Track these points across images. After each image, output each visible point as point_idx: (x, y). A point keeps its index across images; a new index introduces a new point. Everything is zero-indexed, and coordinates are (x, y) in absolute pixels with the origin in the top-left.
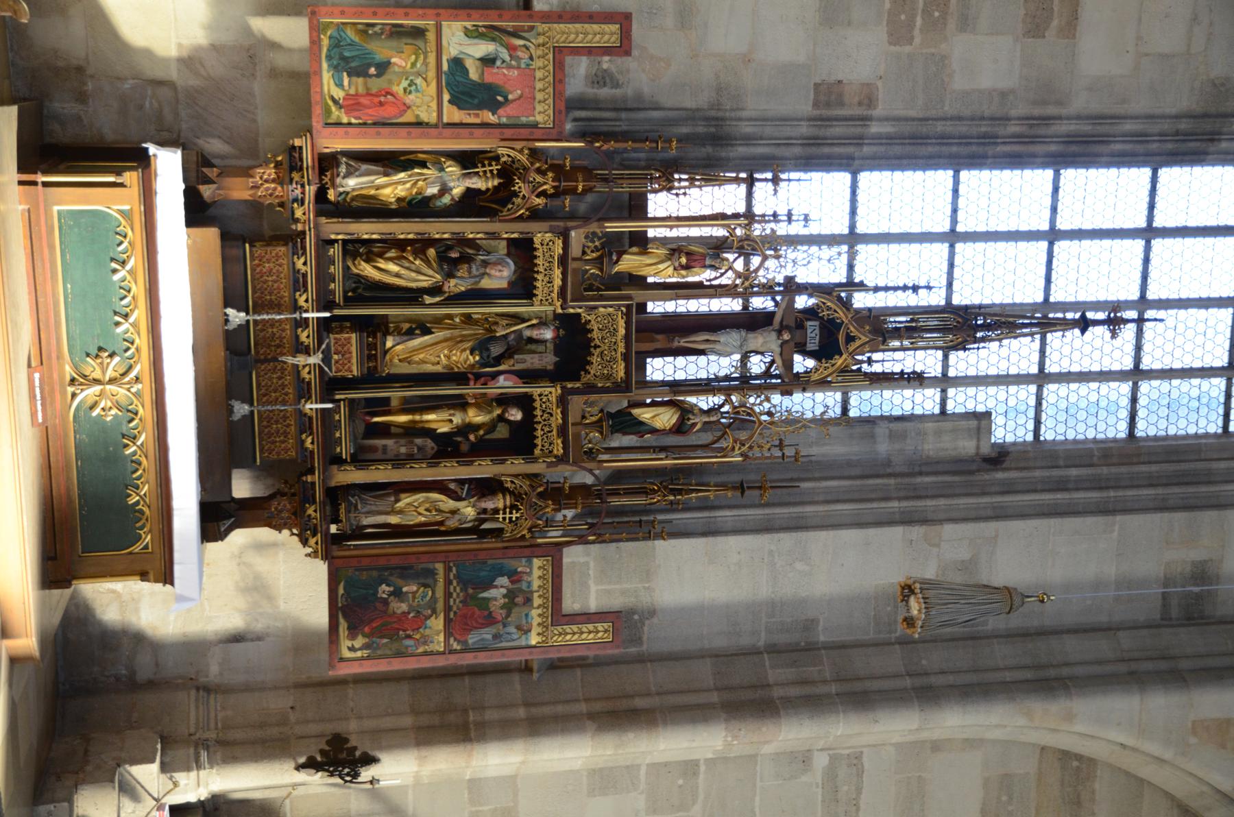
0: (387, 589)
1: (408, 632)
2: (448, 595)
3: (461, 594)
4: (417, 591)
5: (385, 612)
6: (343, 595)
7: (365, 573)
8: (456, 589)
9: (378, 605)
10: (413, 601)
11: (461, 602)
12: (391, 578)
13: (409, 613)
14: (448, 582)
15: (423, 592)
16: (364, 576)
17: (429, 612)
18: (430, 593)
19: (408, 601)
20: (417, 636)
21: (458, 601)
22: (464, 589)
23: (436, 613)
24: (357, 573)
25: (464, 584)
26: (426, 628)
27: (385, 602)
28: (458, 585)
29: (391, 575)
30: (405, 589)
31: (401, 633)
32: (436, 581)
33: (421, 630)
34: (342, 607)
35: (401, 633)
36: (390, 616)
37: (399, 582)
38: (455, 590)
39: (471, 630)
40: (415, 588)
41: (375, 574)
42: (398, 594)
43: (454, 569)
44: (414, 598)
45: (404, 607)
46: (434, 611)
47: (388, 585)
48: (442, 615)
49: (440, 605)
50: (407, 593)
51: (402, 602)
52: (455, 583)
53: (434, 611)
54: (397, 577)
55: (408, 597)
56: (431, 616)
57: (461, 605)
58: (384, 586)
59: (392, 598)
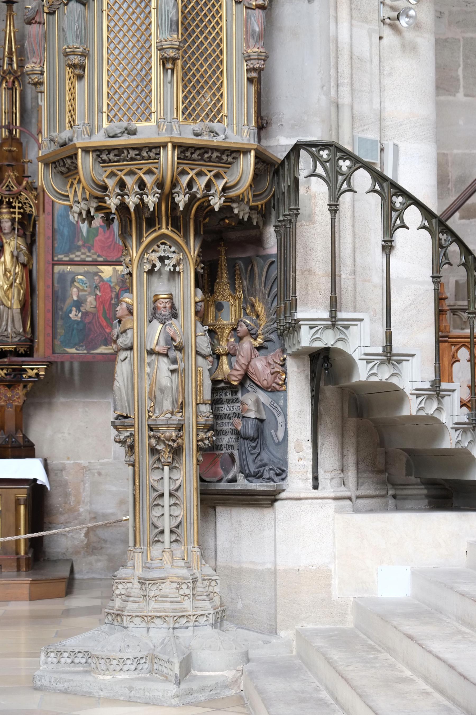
0: (74, 312)
1: (113, 296)
2: (83, 263)
3: (83, 251)
4: (78, 288)
5: (94, 315)
6: (77, 349)
7: (58, 331)
8: (77, 256)
9: (87, 320)
10: (85, 291)
11: (89, 251)
12: (65, 309)
13: (96, 295)
14: (72, 263)
15: (78, 282)
16: (60, 331)
17: (96, 278)
18: (80, 277)
19: (85, 295)
20: (118, 288)
21: (88, 254)
22: (78, 249)
23: (98, 272)
24: (59, 337)
25: (73, 248)
26: (110, 281)
27: (85, 314)
28: (75, 254)
29: (62, 309)
30: (75, 298)
31: (113, 302)
32: (69, 272)
33: (112, 285)
34: (87, 350)
35: (113, 302)
36: (98, 311)
37: (68, 302)
38: (79, 256)
39: (115, 243)
40: (75, 290)
41: (59, 323)
42: (78, 304)
43: (60, 256)
44: (84, 290)
45: (91, 299)
46: (96, 274)
47: (71, 312)
48: (99, 267)
49: (92, 269)
50: (78, 296)
51: (86, 300)
52: (72, 256)
53: (96, 274)
54: (64, 304)
55: (82, 295)
56: (100, 276)
57: (92, 251)
58: (71, 315)
59: (82, 309)
